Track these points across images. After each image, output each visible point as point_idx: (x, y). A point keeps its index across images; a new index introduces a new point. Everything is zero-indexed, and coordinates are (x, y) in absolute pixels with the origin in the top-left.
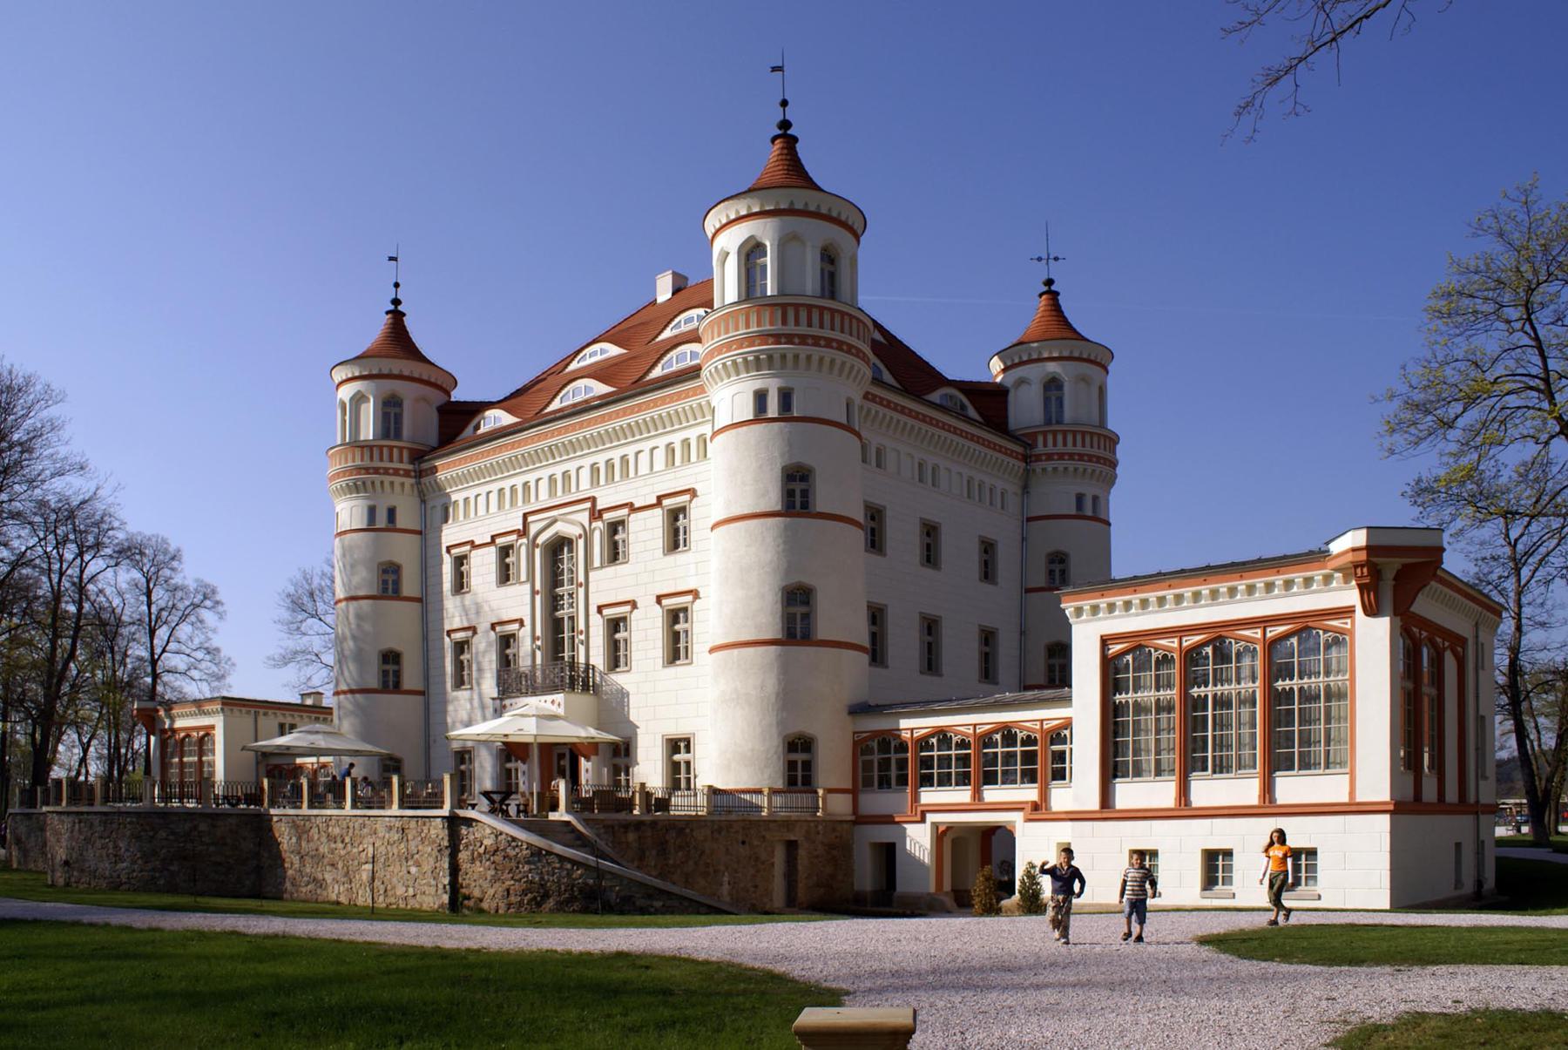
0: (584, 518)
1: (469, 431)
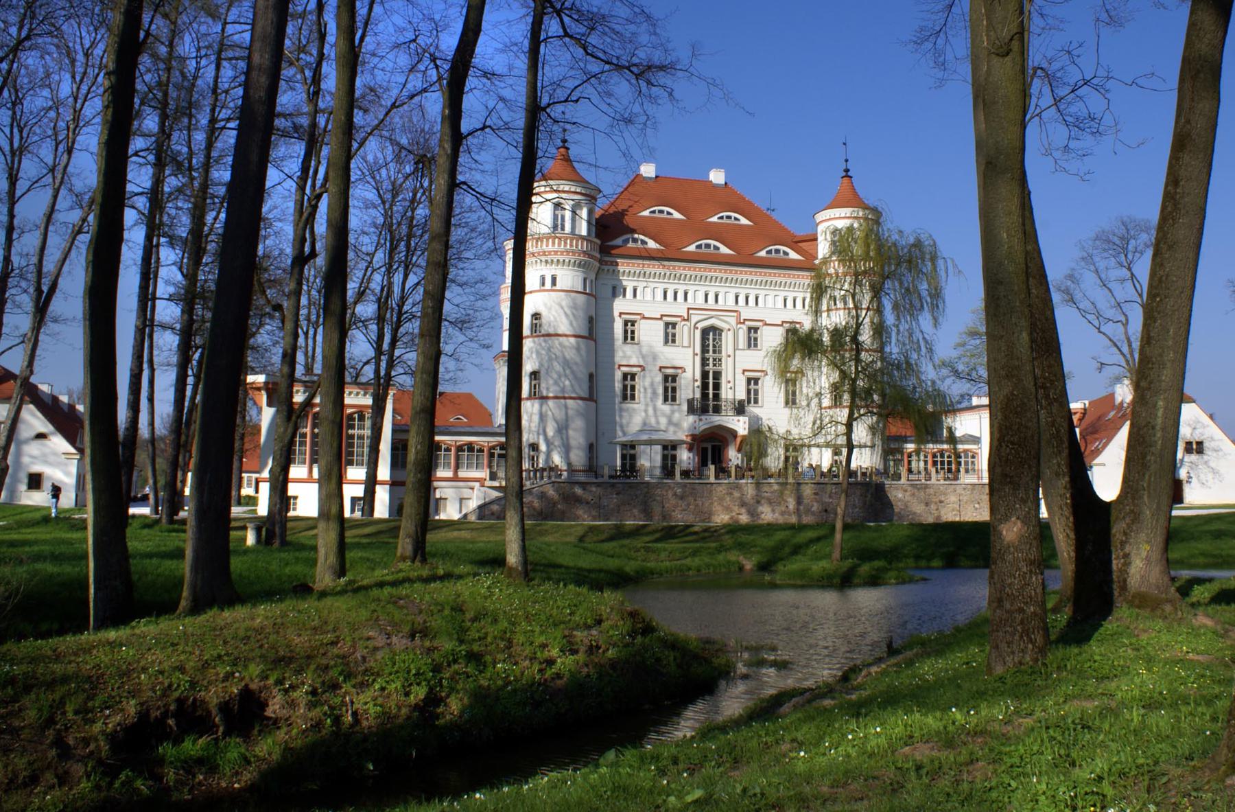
0: (733, 321)
1: (618, 241)
